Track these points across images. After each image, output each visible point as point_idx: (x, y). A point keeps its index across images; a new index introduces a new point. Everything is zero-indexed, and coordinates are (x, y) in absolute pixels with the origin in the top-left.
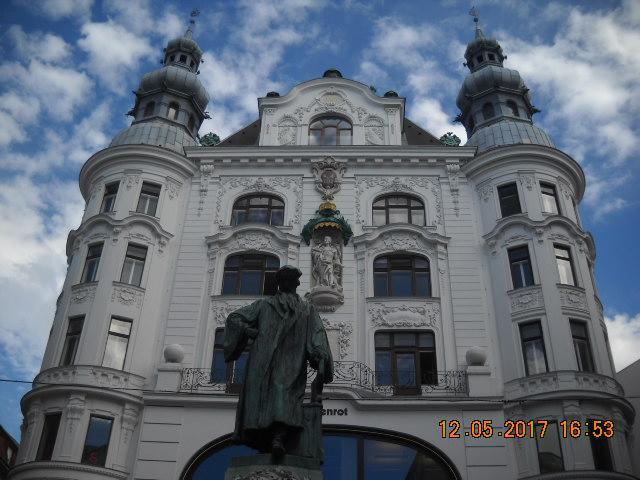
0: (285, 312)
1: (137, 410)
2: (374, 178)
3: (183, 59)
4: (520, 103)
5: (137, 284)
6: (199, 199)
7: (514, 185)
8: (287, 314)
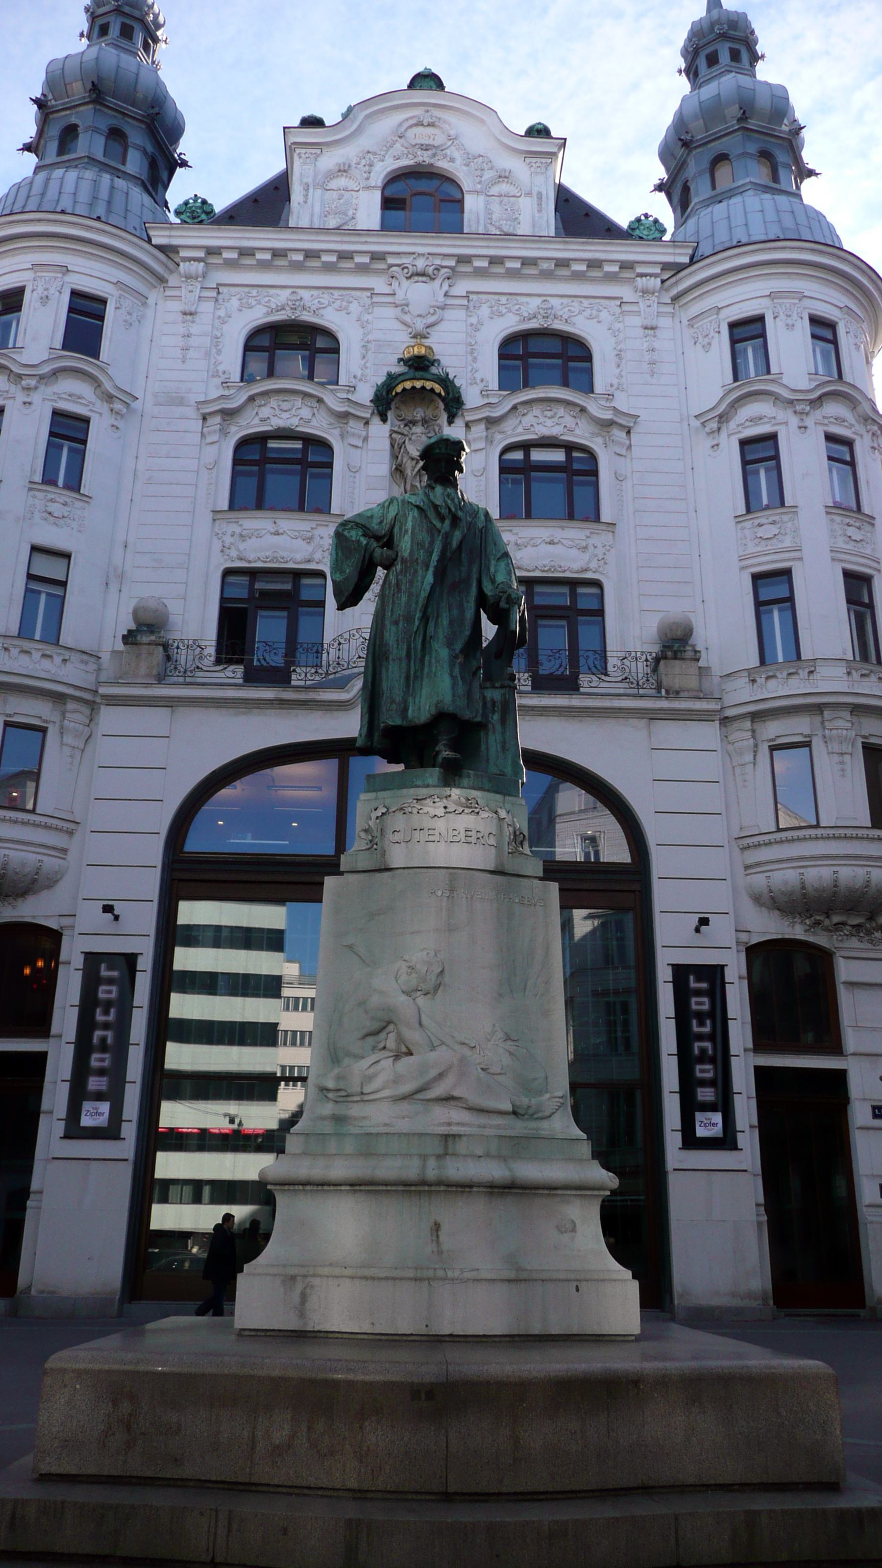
0: (442, 519)
1: (87, 711)
2: (503, 299)
3: (127, 33)
4: (782, 157)
5: (74, 484)
6: (181, 329)
7: (760, 319)
8: (447, 522)
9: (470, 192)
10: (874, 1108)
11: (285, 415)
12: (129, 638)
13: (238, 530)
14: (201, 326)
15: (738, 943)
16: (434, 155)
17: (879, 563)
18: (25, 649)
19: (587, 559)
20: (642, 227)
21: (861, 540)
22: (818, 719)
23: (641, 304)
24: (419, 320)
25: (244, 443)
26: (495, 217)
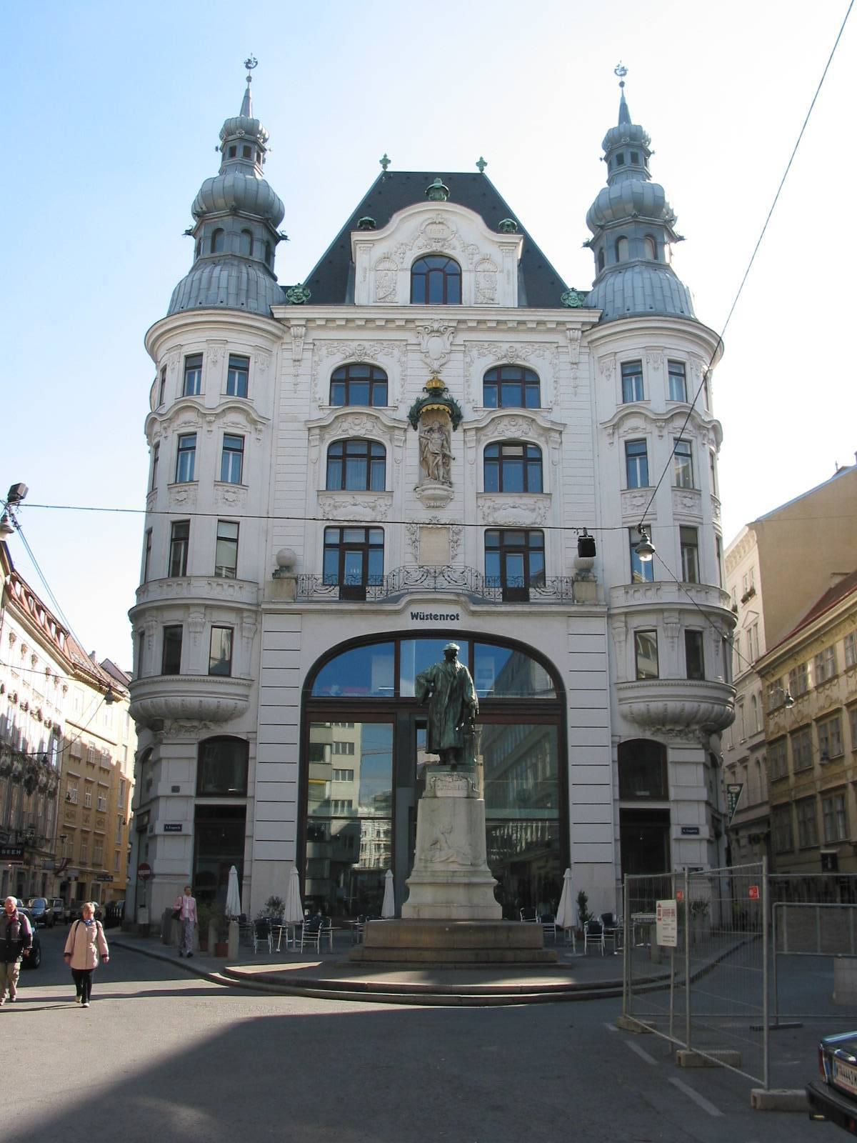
0: (451, 677)
1: (254, 616)
5: (238, 480)
7: (640, 361)
9: (466, 271)
10: (683, 829)
11: (357, 428)
12: (276, 574)
13: (332, 502)
14: (305, 368)
15: (613, 742)
16: (443, 246)
17: (702, 518)
18: (220, 583)
19: (534, 517)
20: (570, 298)
21: (692, 506)
22: (661, 616)
23: (569, 348)
24: (435, 362)
25: (333, 444)
26: (482, 286)
